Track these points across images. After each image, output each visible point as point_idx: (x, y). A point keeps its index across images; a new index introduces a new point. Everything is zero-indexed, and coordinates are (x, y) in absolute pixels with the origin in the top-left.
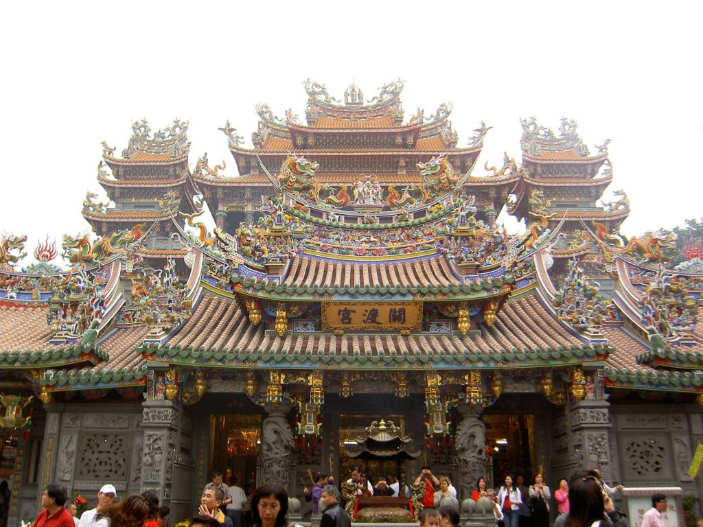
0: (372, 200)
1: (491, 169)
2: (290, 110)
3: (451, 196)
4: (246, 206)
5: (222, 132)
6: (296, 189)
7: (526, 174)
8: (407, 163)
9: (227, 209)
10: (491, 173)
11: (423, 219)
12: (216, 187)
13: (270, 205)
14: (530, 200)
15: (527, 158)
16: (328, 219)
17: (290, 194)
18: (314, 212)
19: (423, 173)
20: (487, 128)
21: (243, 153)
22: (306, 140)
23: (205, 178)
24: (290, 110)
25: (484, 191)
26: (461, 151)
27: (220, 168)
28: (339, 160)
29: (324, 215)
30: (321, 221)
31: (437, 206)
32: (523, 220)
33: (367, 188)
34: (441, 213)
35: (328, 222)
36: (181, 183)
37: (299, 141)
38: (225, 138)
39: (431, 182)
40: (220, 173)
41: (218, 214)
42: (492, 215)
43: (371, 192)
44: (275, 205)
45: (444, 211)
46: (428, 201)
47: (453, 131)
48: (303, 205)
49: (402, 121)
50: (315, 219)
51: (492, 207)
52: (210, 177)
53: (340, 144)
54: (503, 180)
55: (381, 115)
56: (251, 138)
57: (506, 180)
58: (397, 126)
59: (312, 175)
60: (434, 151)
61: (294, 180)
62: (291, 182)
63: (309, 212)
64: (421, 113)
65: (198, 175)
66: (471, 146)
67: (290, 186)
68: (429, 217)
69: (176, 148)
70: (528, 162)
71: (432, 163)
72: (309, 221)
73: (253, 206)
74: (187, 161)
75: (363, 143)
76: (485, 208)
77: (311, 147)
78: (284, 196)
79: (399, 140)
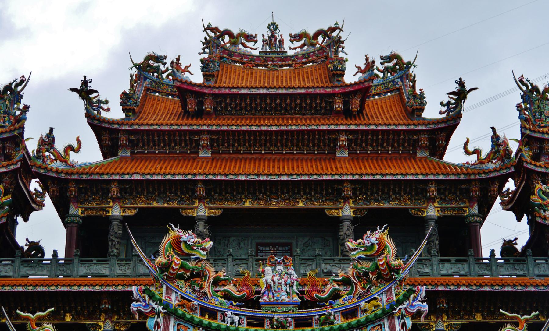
0: (285, 294)
1: (473, 153)
2: (178, 60)
3: (393, 288)
4: (111, 207)
5: (76, 95)
6: (181, 277)
7: (527, 156)
8: (349, 140)
9: (82, 213)
10: (473, 159)
11: (353, 321)
12: (67, 181)
13: (145, 301)
14: (532, 197)
15: (528, 132)
16: (224, 321)
17: (172, 285)
18: (204, 311)
19: (355, 255)
20: (467, 89)
21: (107, 125)
22: (200, 104)
23: (49, 167)
24: (178, 60)
25: (463, 186)
26: (429, 124)
27: (72, 149)
28: (250, 137)
29: (219, 317)
30: (214, 324)
31: (374, 302)
32: (525, 219)
33: (278, 277)
34: (379, 312)
35: (223, 325)
36: (12, 167)
37: (192, 106)
38: (81, 104)
39: (366, 266)
40: (73, 157)
41: (70, 219)
42: (476, 222)
43: (282, 281)
44: (151, 302)
45: (383, 310)
46: (360, 296)
47: (418, 92)
48: (190, 301)
49: (343, 75)
50: (206, 320)
51: (475, 210)
52: (57, 165)
53: (251, 110)
54: (490, 172)
55: (313, 62)
56: (120, 101)
57: (495, 170)
58: (337, 83)
59: (202, 258)
60: (390, 125)
61: (178, 267)
62: (174, 269)
63: (198, 311)
64: (370, 65)
65: (39, 162)
66: (444, 116)
67: (172, 274)
68: (362, 318)
69: (5, 112)
70: (529, 136)
71: (366, 242)
72: (198, 325)
73: (121, 207)
74: (22, 134)
75: (286, 108)
76: (465, 211)
77: (208, 115)
78: (164, 287)
79: (339, 106)
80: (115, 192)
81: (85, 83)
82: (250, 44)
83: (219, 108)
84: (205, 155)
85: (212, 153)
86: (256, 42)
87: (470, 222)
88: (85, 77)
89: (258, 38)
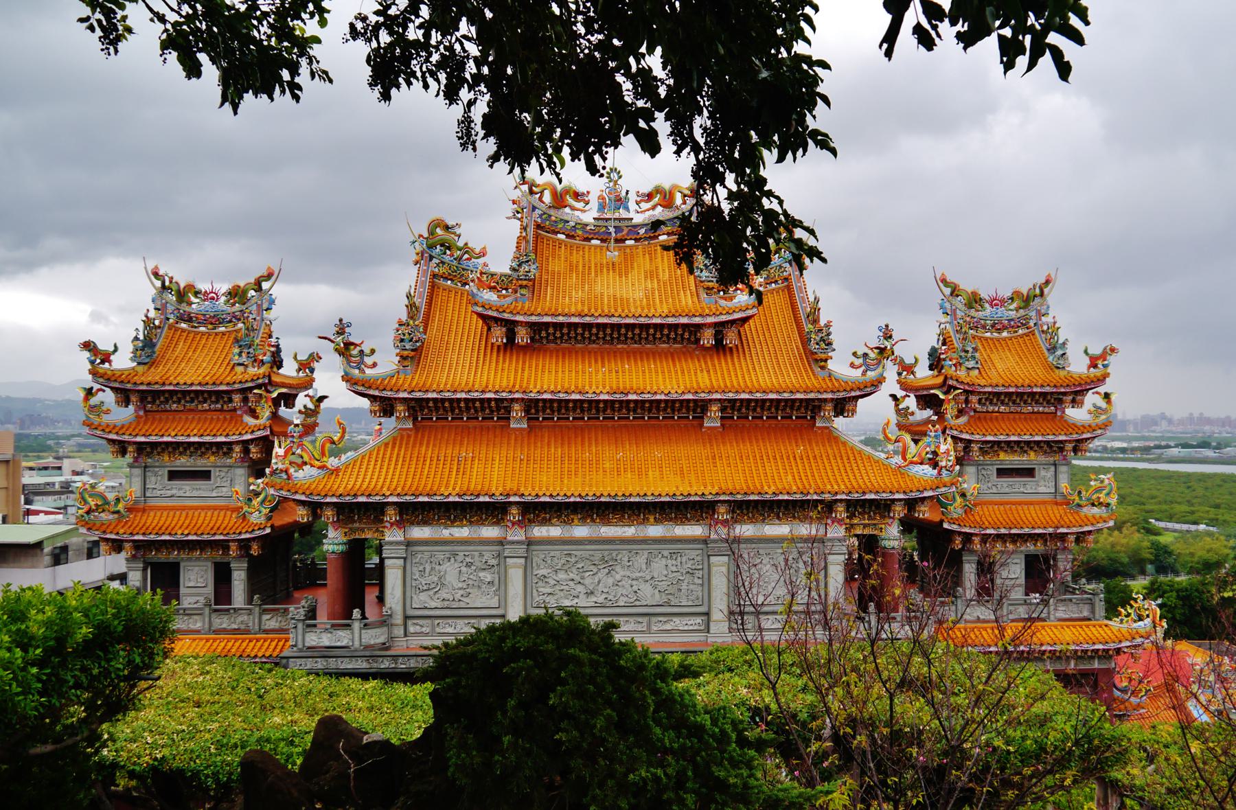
8: (723, 410)
22: (511, 335)
37: (498, 335)
77: (524, 349)
79: (708, 339)
80: (391, 515)
81: (341, 329)
82: (580, 205)
83: (537, 337)
84: (518, 426)
85: (529, 419)
86: (587, 203)
88: (341, 320)
89: (590, 197)
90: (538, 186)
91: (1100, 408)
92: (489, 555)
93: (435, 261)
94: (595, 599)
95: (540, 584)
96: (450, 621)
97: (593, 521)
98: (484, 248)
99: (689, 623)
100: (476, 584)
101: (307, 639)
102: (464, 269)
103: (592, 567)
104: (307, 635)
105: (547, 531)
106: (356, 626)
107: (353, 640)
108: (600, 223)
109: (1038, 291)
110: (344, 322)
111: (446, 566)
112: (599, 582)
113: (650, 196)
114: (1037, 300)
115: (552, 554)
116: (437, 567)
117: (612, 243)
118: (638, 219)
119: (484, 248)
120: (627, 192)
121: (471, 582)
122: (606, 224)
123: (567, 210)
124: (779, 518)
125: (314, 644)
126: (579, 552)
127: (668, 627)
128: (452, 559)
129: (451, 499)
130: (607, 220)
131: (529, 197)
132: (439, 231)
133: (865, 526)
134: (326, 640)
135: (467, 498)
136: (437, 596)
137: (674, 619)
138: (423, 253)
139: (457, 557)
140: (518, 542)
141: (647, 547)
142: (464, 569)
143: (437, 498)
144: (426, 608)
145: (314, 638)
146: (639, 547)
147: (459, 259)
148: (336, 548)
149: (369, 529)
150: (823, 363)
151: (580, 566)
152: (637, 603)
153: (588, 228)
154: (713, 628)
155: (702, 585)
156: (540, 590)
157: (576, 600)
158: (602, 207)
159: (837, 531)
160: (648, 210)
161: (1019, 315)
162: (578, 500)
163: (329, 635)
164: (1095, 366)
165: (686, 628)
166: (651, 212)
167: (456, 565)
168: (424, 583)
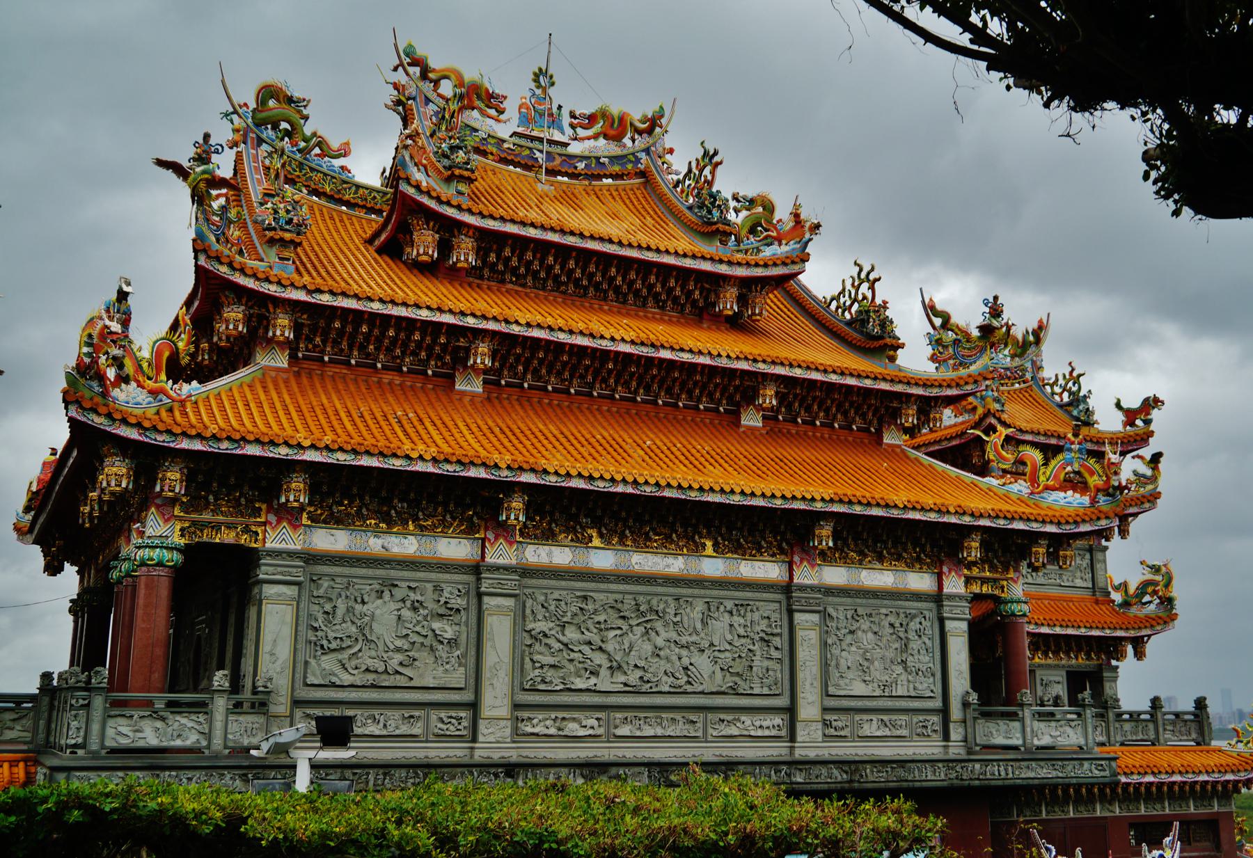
22: (445, 247)
82: (492, 112)
86: (501, 112)
87: (1013, 615)
88: (207, 137)
89: (505, 105)
90: (434, 71)
91: (1144, 476)
92: (453, 590)
93: (264, 147)
94: (622, 679)
95: (537, 647)
96: (376, 713)
97: (622, 542)
98: (347, 144)
99: (765, 724)
100: (427, 642)
101: (110, 732)
102: (312, 169)
103: (620, 623)
104: (111, 722)
105: (549, 554)
106: (220, 704)
107: (209, 736)
108: (523, 142)
109: (1031, 338)
110: (212, 142)
111: (374, 606)
112: (631, 648)
113: (592, 119)
114: (1033, 349)
115: (556, 595)
116: (358, 607)
117: (543, 177)
118: (575, 148)
119: (347, 144)
120: (560, 107)
121: (414, 638)
122: (531, 145)
123: (475, 113)
124: (881, 559)
125: (124, 742)
126: (602, 595)
127: (734, 731)
128: (387, 595)
129: (420, 467)
130: (533, 139)
131: (421, 84)
132: (272, 103)
133: (984, 581)
134: (150, 735)
135: (449, 468)
136: (354, 663)
137: (743, 718)
138: (247, 130)
139: (395, 591)
140: (506, 569)
141: (703, 592)
142: (406, 613)
143: (397, 464)
144: (334, 685)
145: (124, 730)
146: (690, 591)
147: (305, 152)
148: (167, 555)
149: (230, 526)
150: (892, 353)
151: (601, 618)
152: (689, 688)
153: (506, 145)
154: (801, 734)
155: (780, 660)
156: (536, 657)
157: (593, 680)
158: (526, 120)
159: (954, 585)
160: (589, 138)
161: (1015, 364)
162: (630, 490)
163: (159, 724)
164: (1132, 424)
165: (760, 733)
166: (592, 143)
167: (393, 606)
168: (331, 635)
